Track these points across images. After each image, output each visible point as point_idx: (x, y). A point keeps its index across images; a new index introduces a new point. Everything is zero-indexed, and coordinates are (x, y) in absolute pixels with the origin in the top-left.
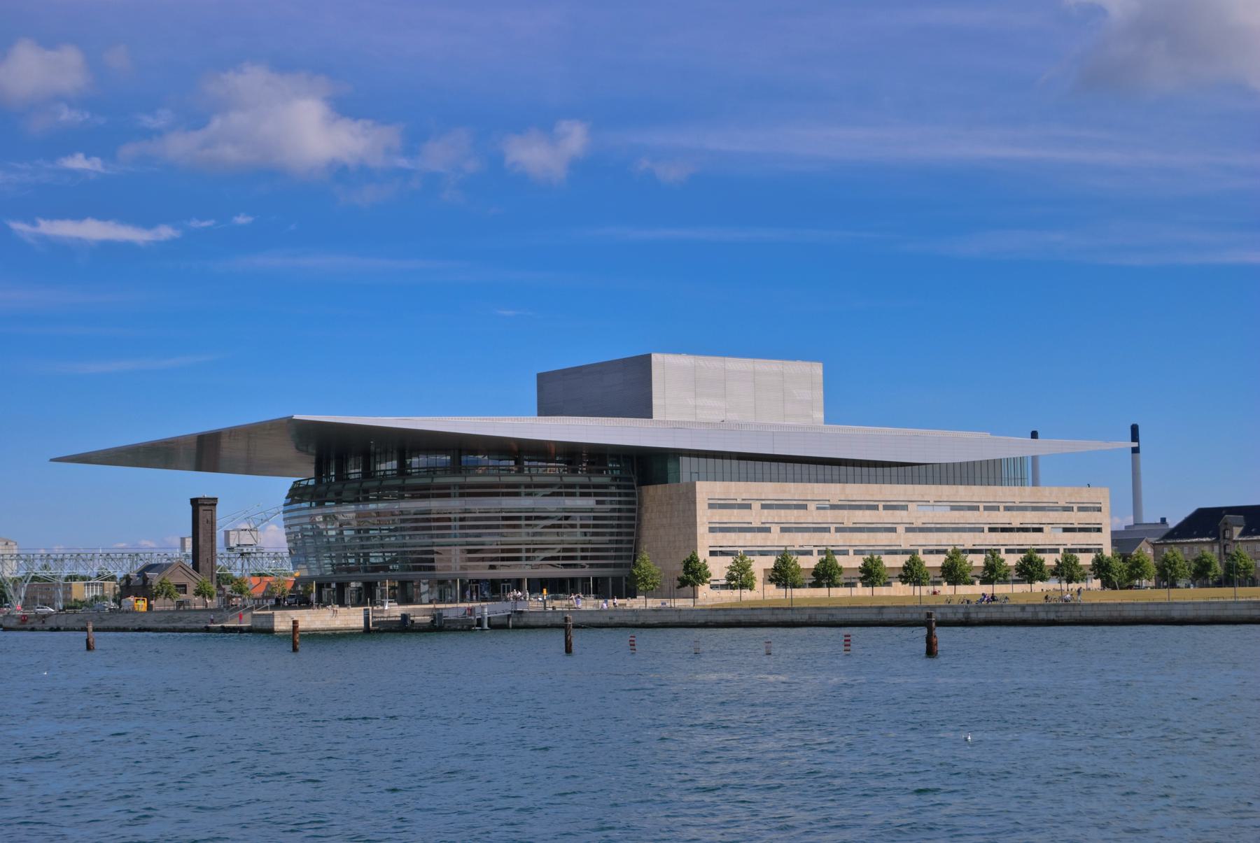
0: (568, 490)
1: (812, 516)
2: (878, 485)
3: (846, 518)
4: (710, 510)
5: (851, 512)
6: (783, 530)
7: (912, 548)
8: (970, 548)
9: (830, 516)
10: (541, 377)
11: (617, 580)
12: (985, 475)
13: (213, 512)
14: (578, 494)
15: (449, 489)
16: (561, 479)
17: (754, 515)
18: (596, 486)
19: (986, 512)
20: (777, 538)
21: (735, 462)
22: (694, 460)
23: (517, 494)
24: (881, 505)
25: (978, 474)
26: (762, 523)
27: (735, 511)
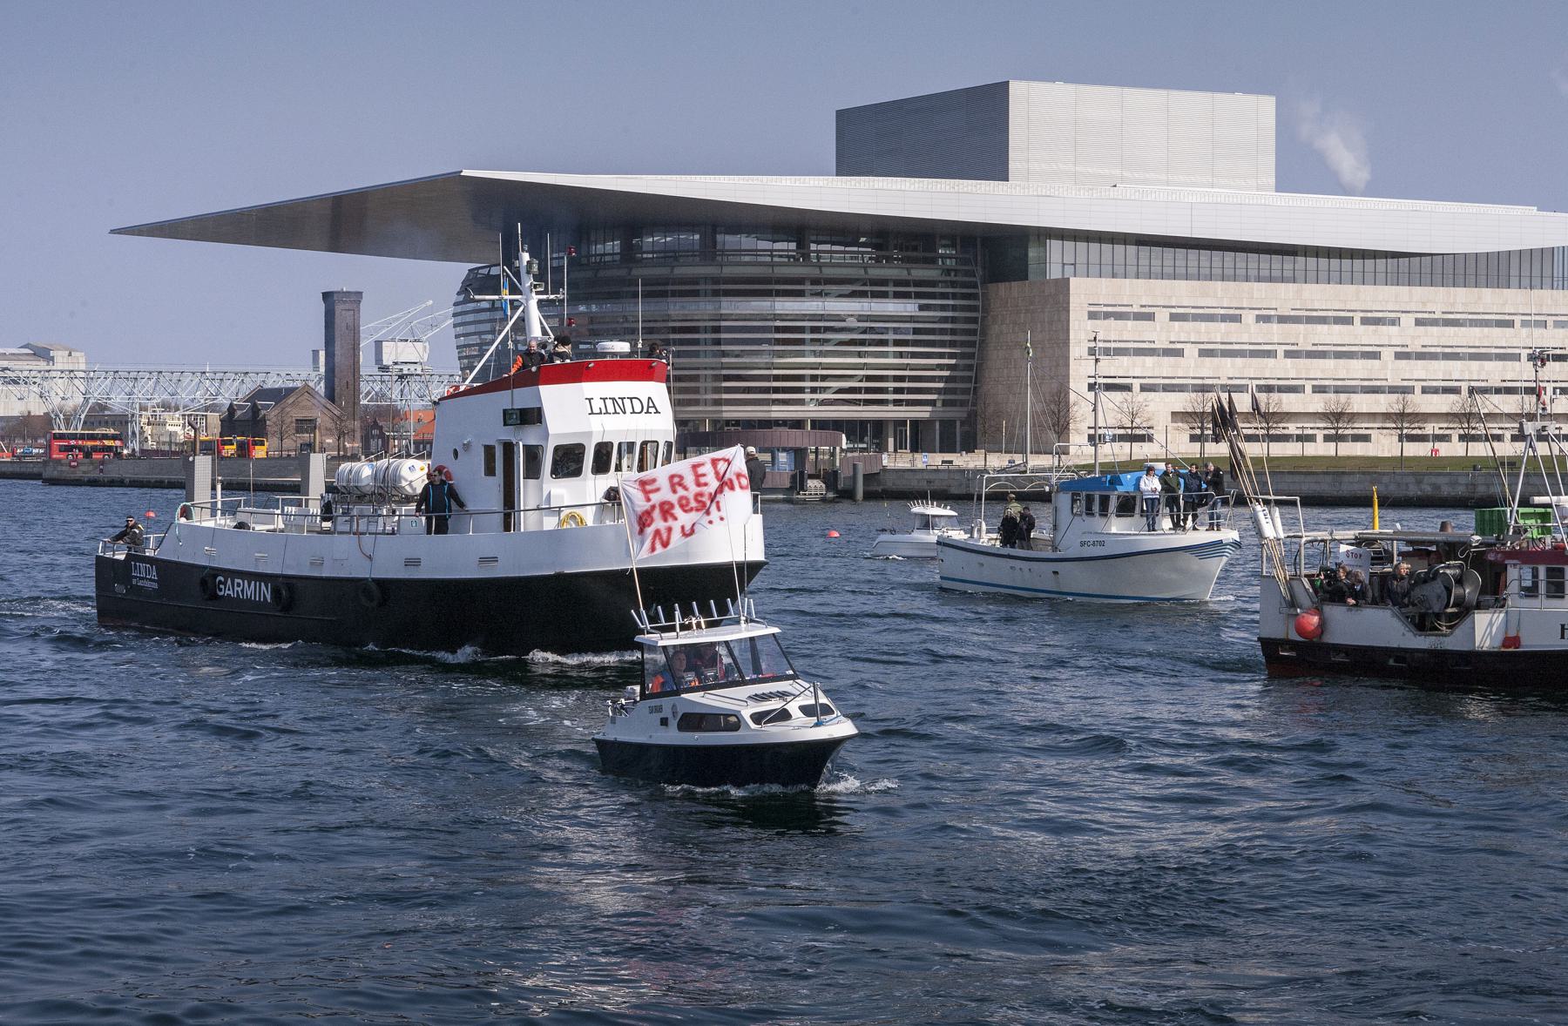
0: (875, 289)
1: (1249, 332)
2: (1354, 287)
4: (1090, 321)
5: (1309, 326)
6: (1204, 353)
7: (1406, 383)
8: (1497, 385)
9: (1276, 332)
10: (841, 114)
11: (948, 425)
12: (1525, 273)
13: (356, 311)
14: (891, 294)
15: (698, 284)
16: (866, 272)
17: (1158, 329)
18: (918, 283)
19: (1525, 331)
21: (1132, 249)
22: (1069, 245)
23: (800, 294)
24: (1357, 317)
25: (1514, 272)
26: (1174, 342)
27: (1130, 323)
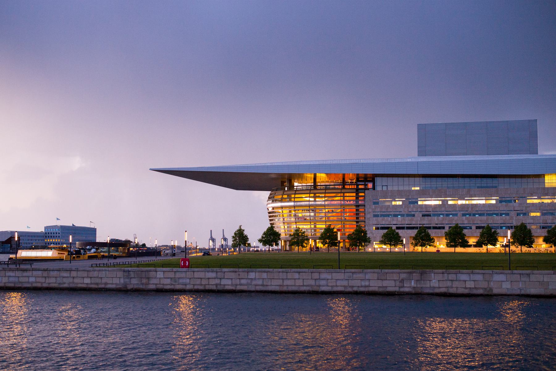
3: (470, 210)
20: (419, 219)
